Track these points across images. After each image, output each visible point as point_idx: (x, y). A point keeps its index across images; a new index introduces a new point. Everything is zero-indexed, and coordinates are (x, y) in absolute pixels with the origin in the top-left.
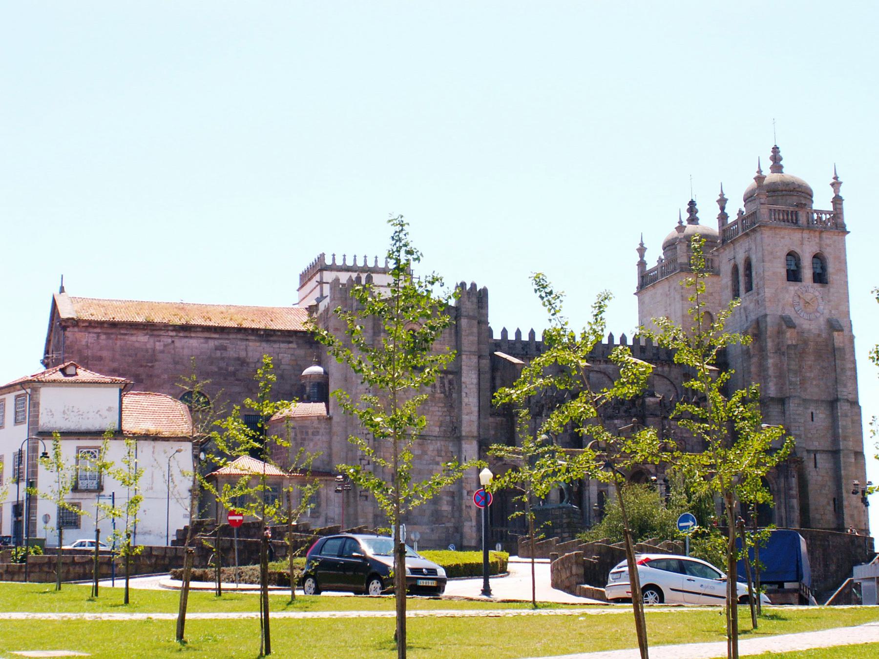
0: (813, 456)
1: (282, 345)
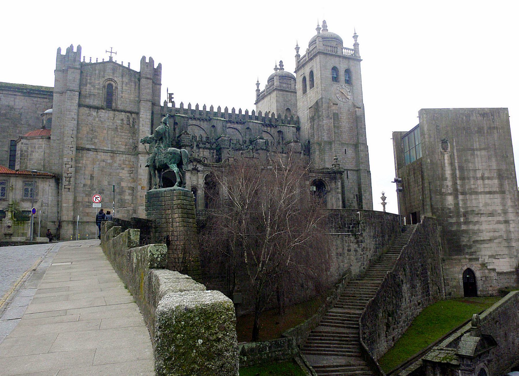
1: (39, 99)
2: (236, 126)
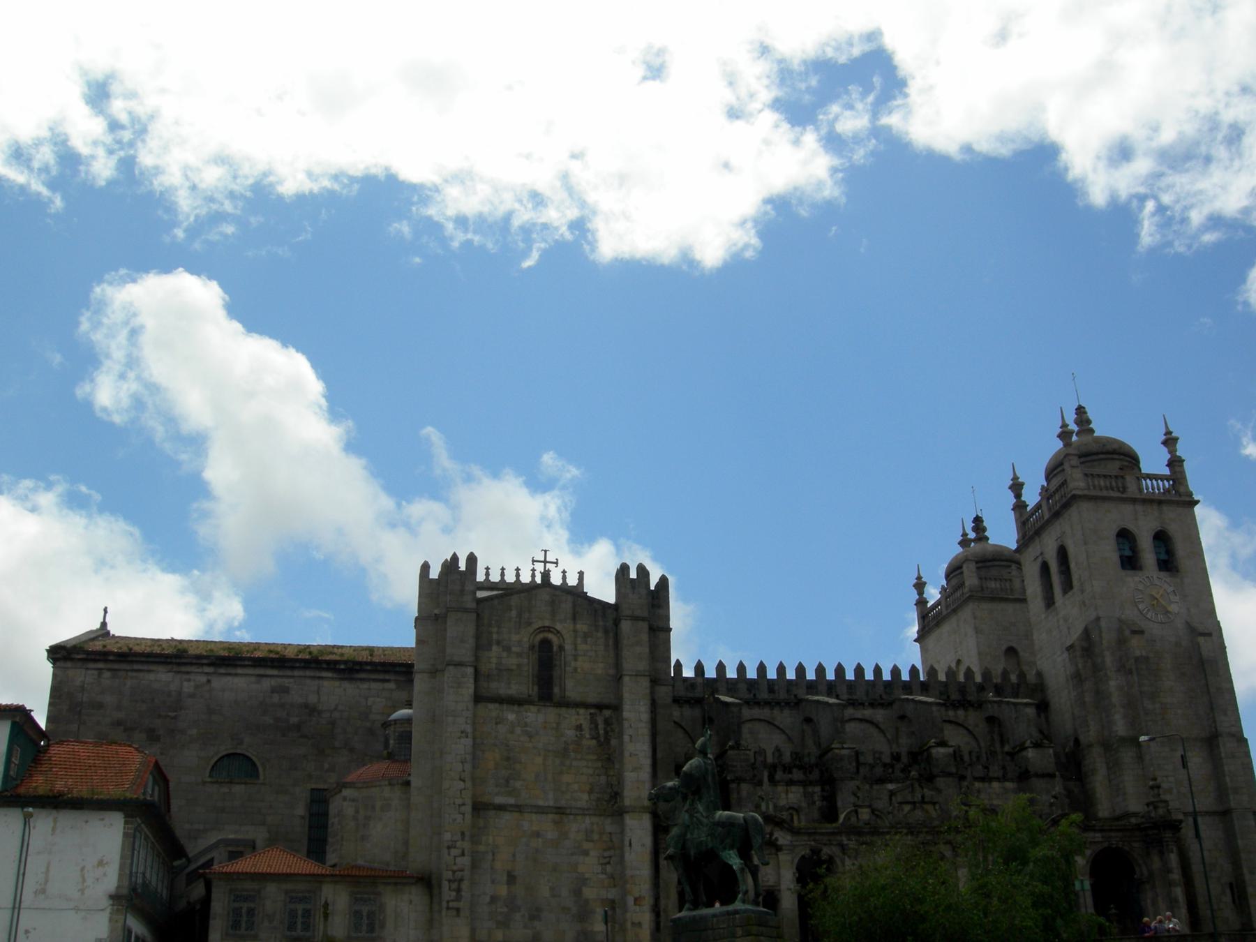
0: (1191, 820)
1: (374, 685)
2: (868, 713)
